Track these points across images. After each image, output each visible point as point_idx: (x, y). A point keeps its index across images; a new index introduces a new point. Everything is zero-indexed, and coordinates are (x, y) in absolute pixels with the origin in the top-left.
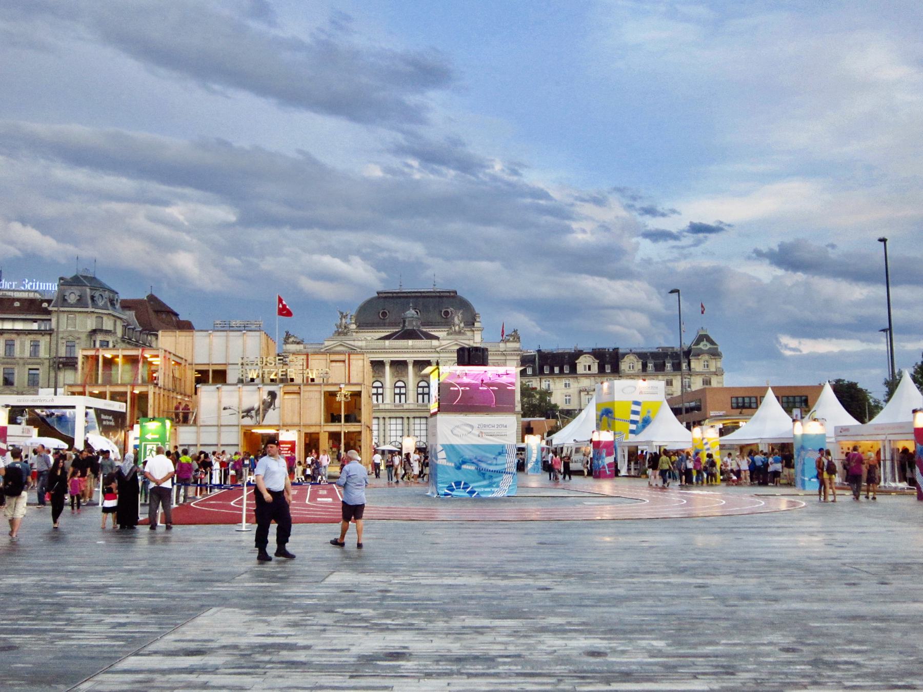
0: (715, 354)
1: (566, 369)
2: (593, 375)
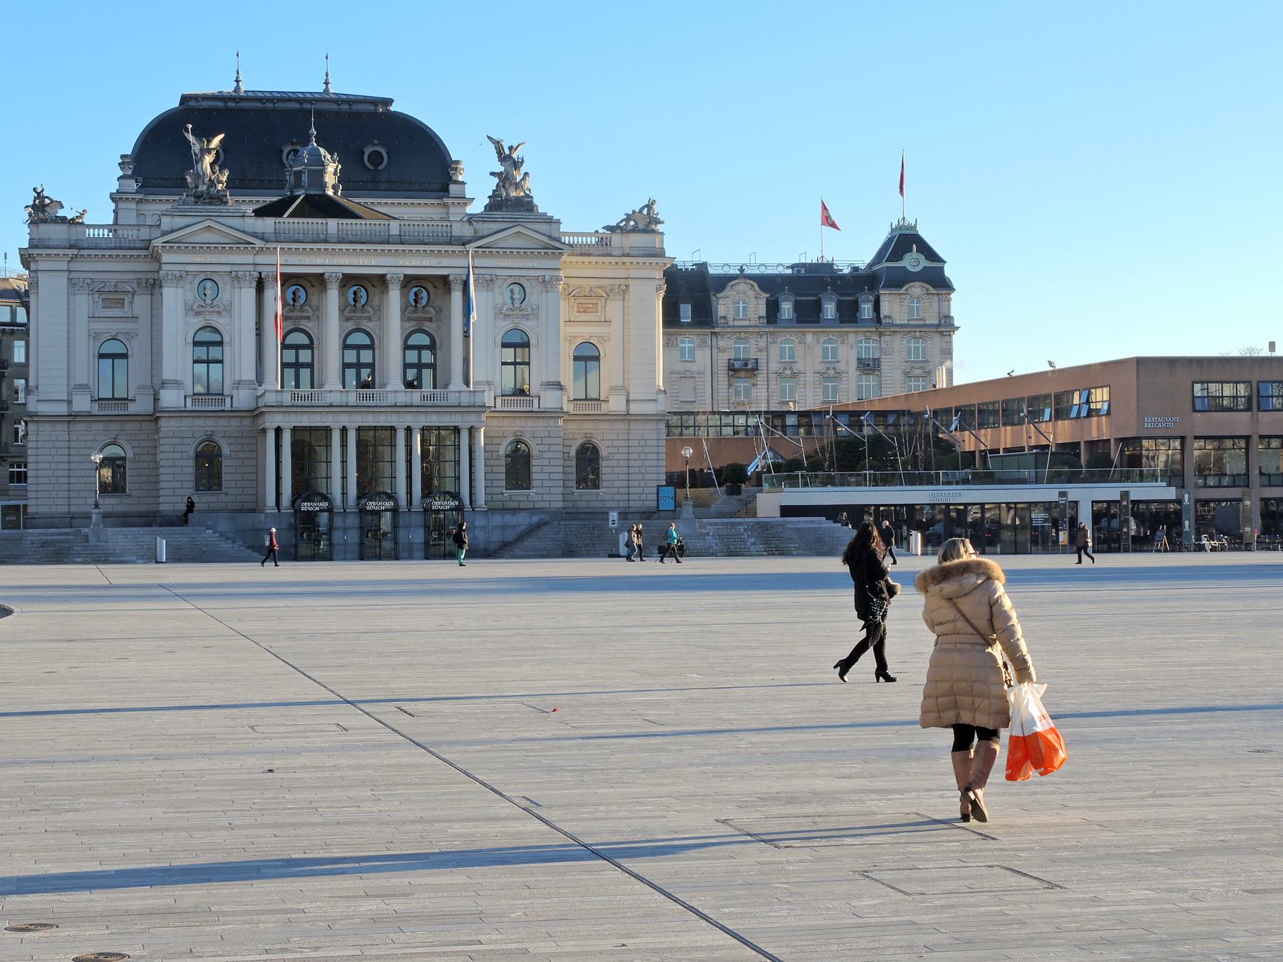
0: (938, 282)
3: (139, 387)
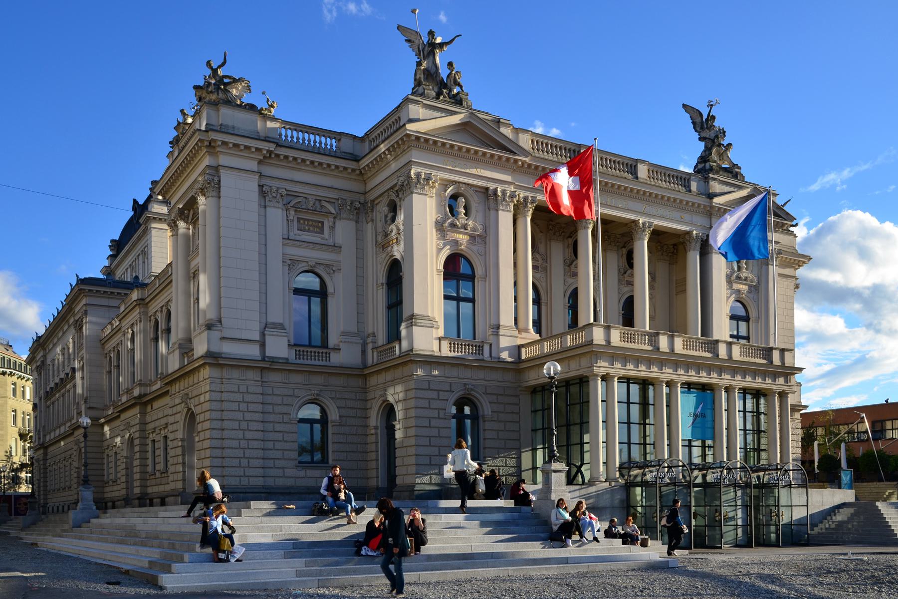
3: (344, 334)
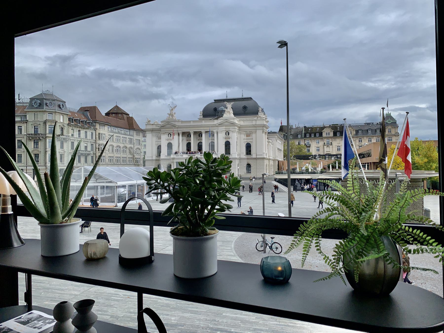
1: (317, 135)
2: (331, 137)
